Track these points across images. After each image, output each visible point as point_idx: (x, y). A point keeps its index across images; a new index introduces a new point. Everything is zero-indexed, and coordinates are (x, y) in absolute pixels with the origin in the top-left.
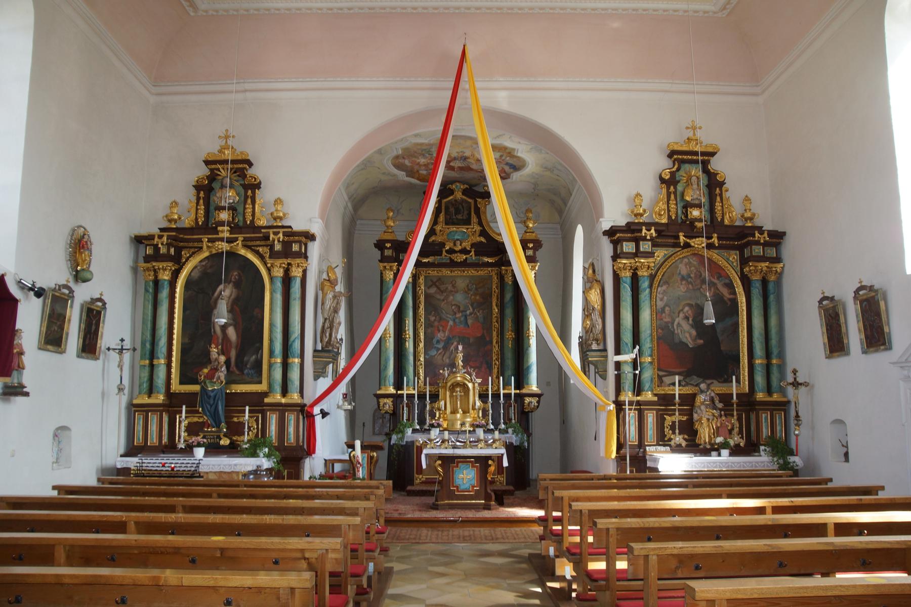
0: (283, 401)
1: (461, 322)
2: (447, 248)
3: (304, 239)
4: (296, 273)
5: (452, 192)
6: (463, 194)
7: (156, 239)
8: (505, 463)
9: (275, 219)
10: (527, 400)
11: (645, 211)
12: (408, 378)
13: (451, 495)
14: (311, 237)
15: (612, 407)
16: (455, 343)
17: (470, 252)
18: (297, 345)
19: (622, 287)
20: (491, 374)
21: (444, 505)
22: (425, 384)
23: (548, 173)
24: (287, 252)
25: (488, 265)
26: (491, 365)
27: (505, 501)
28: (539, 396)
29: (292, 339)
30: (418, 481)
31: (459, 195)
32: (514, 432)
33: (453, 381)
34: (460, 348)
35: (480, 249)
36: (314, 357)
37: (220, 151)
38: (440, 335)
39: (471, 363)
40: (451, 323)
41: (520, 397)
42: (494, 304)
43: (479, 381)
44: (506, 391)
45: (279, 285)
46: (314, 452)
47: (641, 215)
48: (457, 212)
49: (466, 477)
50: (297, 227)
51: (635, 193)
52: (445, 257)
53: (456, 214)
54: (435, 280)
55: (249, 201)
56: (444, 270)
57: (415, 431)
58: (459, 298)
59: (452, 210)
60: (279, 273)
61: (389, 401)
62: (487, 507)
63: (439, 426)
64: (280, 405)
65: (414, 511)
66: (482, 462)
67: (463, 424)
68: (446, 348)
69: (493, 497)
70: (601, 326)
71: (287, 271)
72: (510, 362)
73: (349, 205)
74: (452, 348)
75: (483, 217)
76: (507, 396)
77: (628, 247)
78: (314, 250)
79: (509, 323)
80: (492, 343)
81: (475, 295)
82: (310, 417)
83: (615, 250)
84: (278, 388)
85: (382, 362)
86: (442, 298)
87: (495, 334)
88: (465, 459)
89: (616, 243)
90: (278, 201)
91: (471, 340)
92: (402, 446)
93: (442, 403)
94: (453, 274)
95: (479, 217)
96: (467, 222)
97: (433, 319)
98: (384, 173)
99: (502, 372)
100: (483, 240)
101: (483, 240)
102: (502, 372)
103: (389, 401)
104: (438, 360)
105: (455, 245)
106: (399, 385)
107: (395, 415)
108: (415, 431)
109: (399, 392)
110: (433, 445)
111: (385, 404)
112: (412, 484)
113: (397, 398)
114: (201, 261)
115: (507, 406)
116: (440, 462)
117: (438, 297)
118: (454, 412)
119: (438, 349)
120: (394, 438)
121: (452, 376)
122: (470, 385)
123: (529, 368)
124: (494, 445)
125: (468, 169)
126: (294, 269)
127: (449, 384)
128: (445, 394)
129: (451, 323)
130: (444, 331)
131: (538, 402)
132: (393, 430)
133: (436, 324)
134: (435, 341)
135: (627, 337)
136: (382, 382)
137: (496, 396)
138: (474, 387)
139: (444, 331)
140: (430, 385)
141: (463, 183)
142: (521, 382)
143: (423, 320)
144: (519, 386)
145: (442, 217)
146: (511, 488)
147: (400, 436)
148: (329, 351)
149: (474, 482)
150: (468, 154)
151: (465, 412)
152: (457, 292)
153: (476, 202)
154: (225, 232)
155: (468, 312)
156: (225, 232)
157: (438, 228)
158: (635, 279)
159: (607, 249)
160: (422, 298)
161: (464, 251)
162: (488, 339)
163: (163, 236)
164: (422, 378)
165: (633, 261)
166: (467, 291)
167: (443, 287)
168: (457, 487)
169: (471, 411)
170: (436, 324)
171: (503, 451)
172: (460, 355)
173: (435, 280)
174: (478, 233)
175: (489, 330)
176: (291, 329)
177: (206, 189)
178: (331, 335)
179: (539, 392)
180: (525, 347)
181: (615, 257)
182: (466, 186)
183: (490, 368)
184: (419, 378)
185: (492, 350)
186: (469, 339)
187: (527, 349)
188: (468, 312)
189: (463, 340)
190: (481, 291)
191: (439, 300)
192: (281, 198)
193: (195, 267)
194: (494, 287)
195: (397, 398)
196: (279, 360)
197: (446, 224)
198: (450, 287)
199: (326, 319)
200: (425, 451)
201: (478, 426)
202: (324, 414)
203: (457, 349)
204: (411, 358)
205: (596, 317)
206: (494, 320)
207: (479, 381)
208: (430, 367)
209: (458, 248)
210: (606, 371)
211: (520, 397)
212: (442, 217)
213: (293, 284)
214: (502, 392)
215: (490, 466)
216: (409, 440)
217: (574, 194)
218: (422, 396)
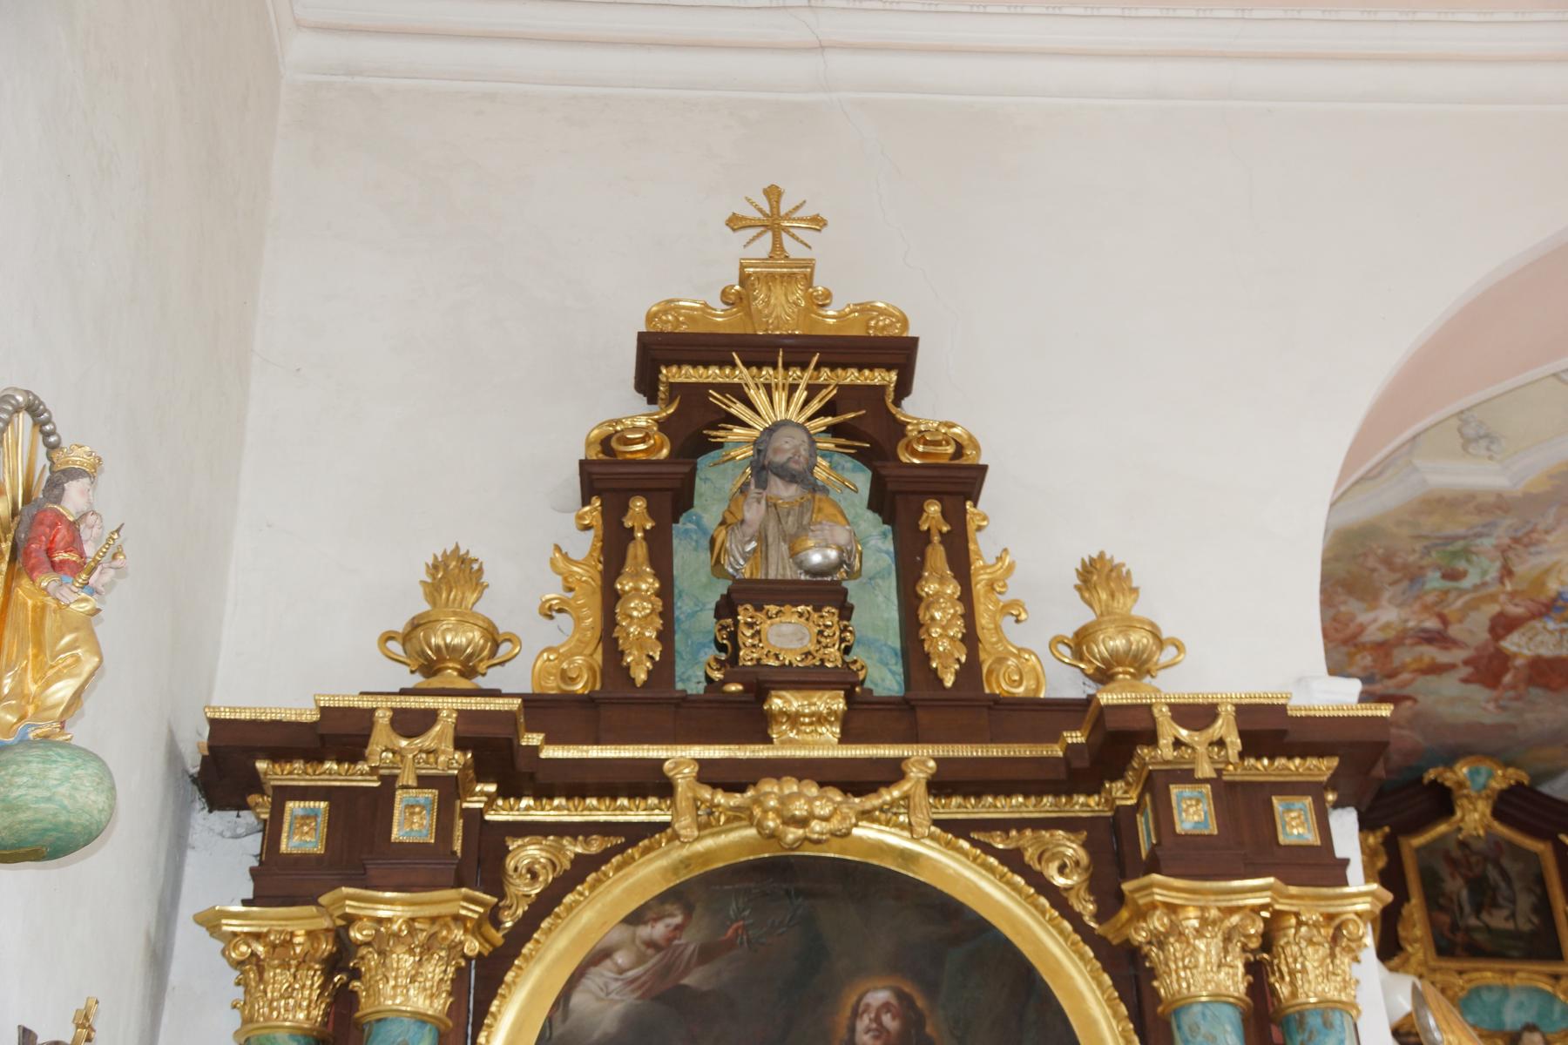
6: (1497, 814)
7: (383, 745)
31: (1474, 817)
37: (738, 299)
48: (1483, 894)
55: (937, 555)
59: (1455, 886)
114: (635, 918)
154: (809, 728)
156: (809, 728)
163: (428, 718)
177: (637, 494)
182: (1515, 775)
192: (1117, 555)
193: (600, 956)
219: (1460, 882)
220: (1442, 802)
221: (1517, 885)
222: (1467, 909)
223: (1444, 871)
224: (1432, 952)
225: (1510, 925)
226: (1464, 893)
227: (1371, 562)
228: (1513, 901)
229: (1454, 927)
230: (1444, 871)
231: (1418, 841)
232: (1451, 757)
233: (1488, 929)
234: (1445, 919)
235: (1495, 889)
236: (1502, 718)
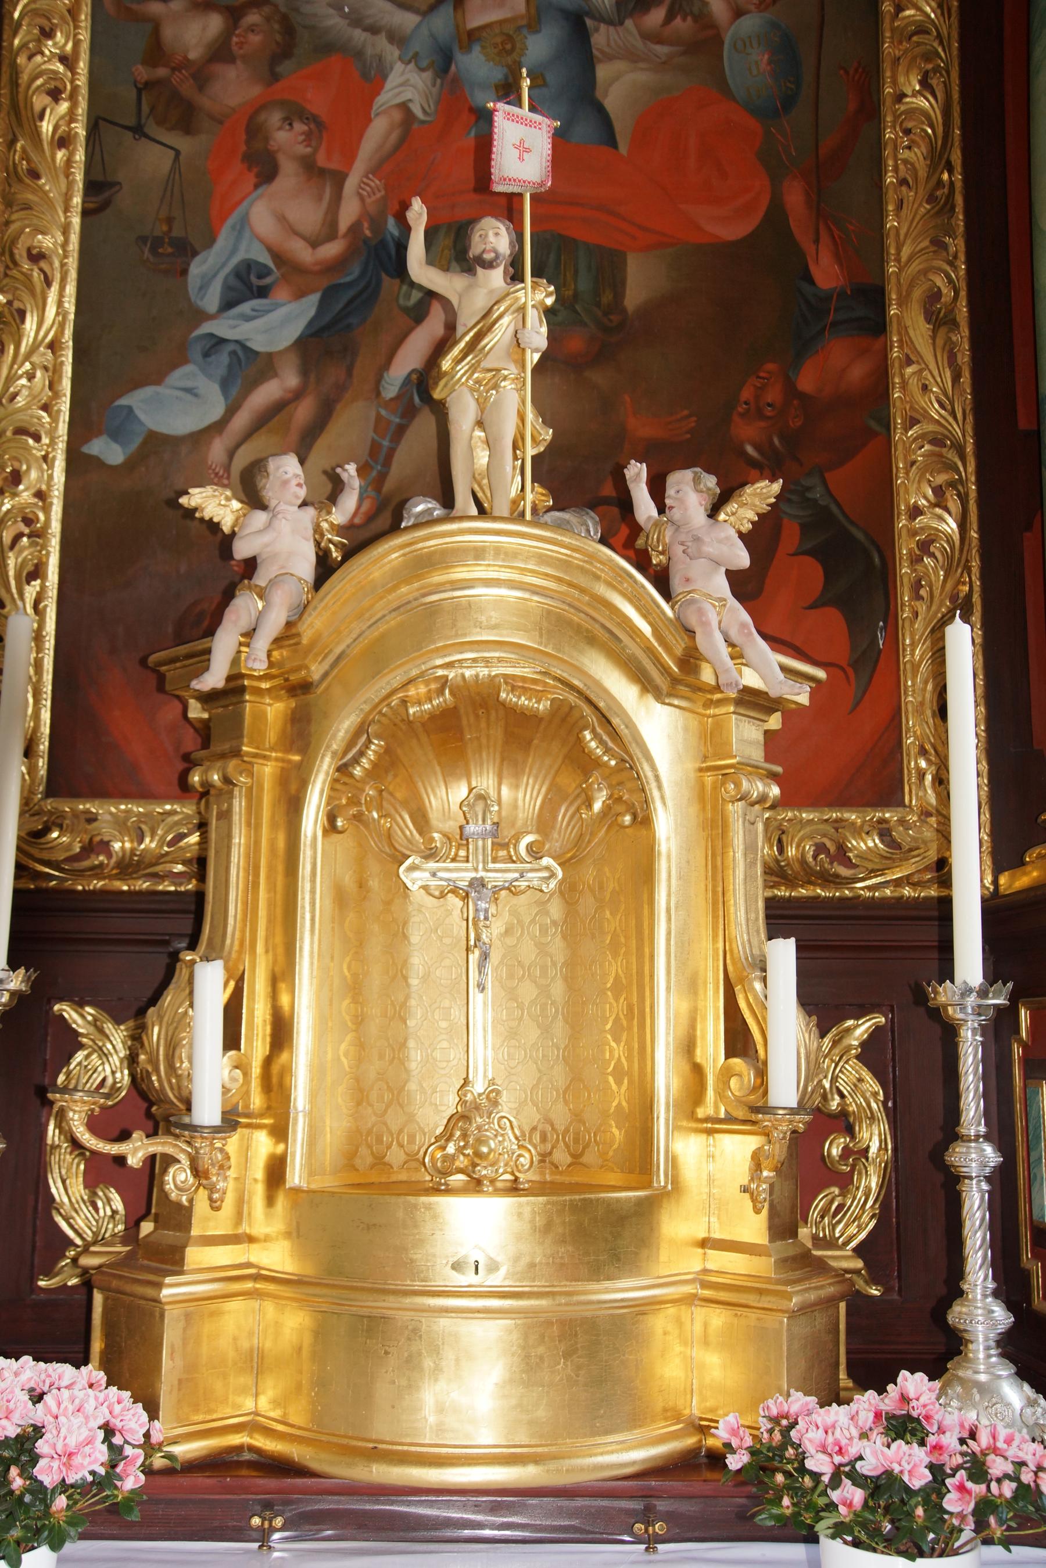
38: (271, 218)
40: (406, 86)
80: (866, 310)
87: (904, 224)
91: (641, 282)
119: (246, 367)
129: (406, 86)
134: (208, 272)
139: (324, 177)
162: (827, 273)
170: (234, 89)
175: (843, 157)
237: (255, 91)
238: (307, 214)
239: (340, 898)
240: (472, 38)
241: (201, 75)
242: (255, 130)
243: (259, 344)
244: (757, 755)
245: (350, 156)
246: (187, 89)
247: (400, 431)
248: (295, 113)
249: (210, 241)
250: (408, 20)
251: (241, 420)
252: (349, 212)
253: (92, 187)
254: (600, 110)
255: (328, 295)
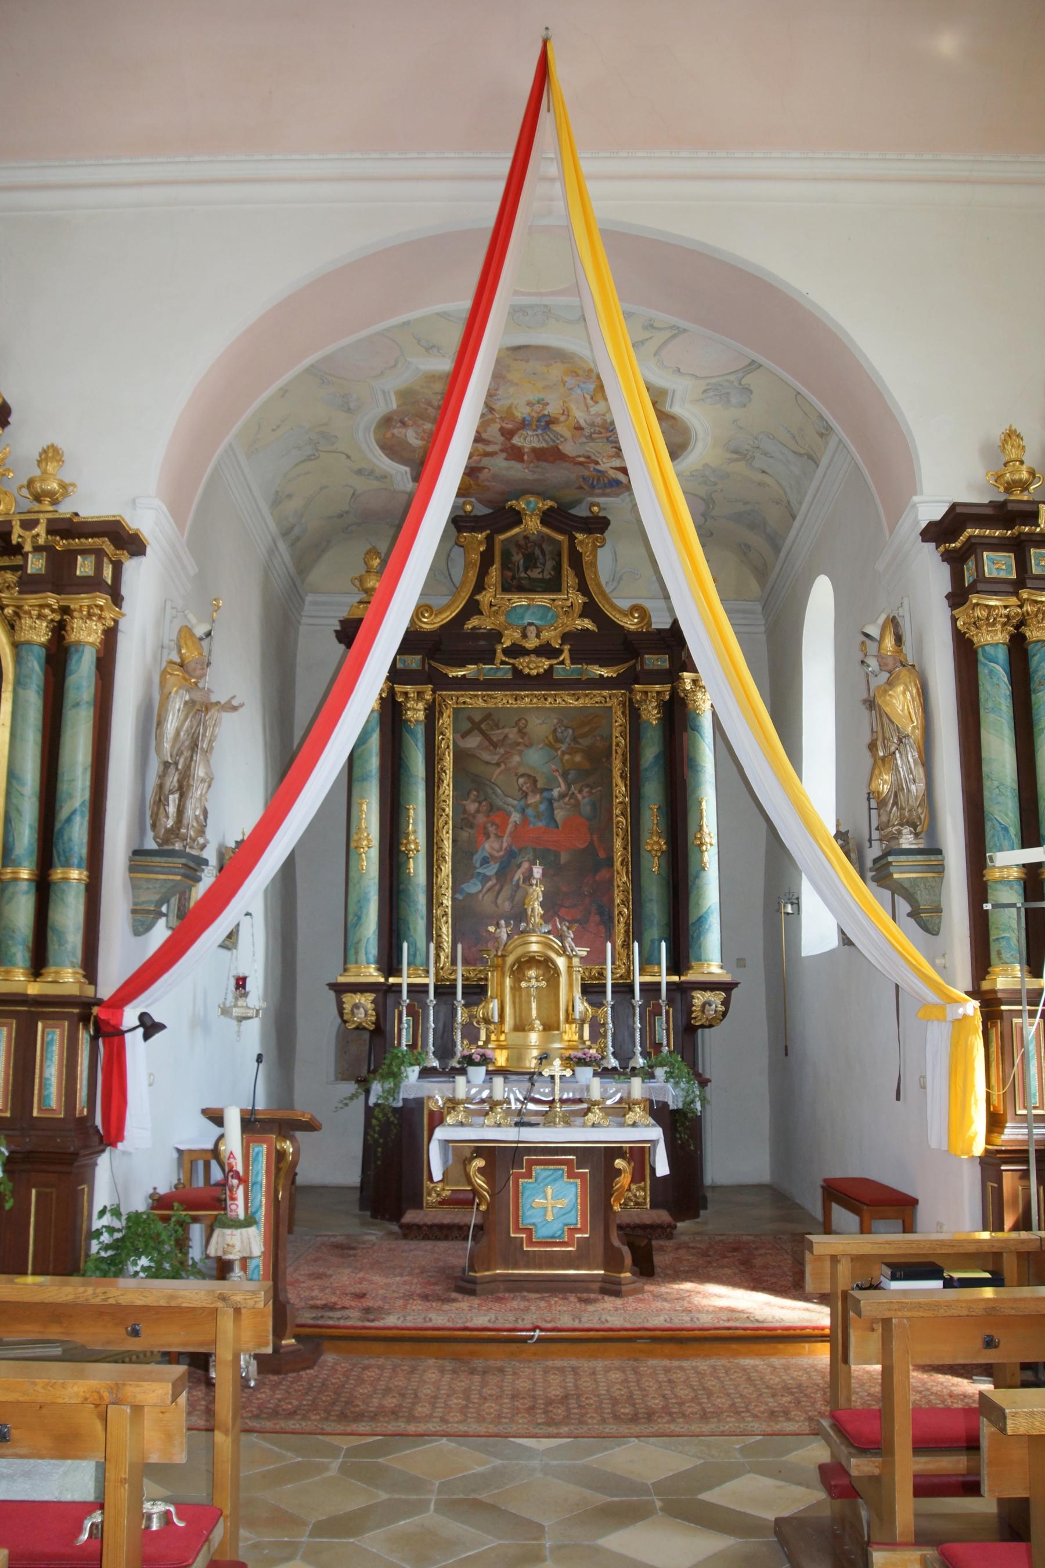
0: (33, 989)
1: (538, 816)
2: (507, 643)
3: (108, 547)
4: (86, 634)
5: (516, 518)
8: (662, 1168)
9: (38, 498)
10: (699, 998)
11: (1032, 473)
12: (413, 946)
13: (514, 1254)
14: (131, 544)
15: (972, 1007)
16: (526, 865)
17: (560, 652)
18: (77, 833)
19: (983, 672)
20: (610, 937)
21: (495, 1279)
22: (454, 962)
23: (740, 467)
24: (60, 577)
25: (602, 683)
26: (611, 918)
27: (658, 1259)
28: (727, 988)
29: (63, 814)
30: (433, 1198)
31: (533, 525)
32: (670, 1075)
33: (519, 951)
34: (537, 871)
35: (583, 647)
36: (133, 869)
38: (490, 846)
39: (563, 912)
40: (515, 817)
41: (681, 992)
42: (616, 773)
43: (583, 952)
44: (648, 979)
45: (35, 667)
46: (119, 1136)
47: (1024, 486)
48: (531, 561)
49: (552, 1205)
50: (90, 505)
51: (1004, 428)
52: (499, 668)
53: (526, 570)
54: (477, 718)
56: (498, 693)
57: (426, 1073)
58: (535, 758)
59: (518, 558)
60: (38, 633)
61: (366, 1000)
62: (611, 1289)
63: (485, 1060)
64: (22, 999)
65: (408, 1297)
66: (599, 1163)
67: (544, 1058)
68: (504, 873)
69: (628, 1259)
70: (922, 785)
71: (59, 630)
72: (655, 909)
73: (282, 546)
74: (519, 875)
75: (589, 575)
76: (651, 990)
77: (998, 565)
78: (141, 579)
79: (652, 818)
80: (610, 862)
81: (572, 751)
82: (109, 1035)
83: (957, 577)
84: (21, 954)
85: (352, 908)
86: (495, 759)
87: (618, 844)
88: (549, 1153)
89: (955, 560)
90: (51, 454)
91: (564, 858)
92: (395, 1110)
93: (494, 1005)
94: (521, 704)
95: (580, 574)
96: (554, 585)
97: (472, 807)
98: (360, 472)
99: (636, 931)
100: (588, 624)
101: (588, 624)
102: (636, 931)
103: (366, 1000)
104: (486, 902)
105: (524, 636)
106: (390, 964)
107: (380, 1033)
108: (426, 1073)
109: (392, 980)
110: (466, 1117)
111: (356, 1006)
112: (417, 1203)
113: (385, 993)
115: (651, 1012)
116: (480, 1163)
117: (486, 756)
118: (522, 1026)
119: (485, 879)
120: (377, 1088)
121: (517, 939)
122: (561, 962)
123: (701, 920)
124: (631, 1117)
125: (552, 455)
126: (77, 623)
127: (510, 960)
128: (502, 984)
129: (515, 817)
130: (499, 837)
131: (726, 1003)
132: (374, 1072)
133: (481, 819)
134: (477, 858)
135: (1003, 808)
136: (351, 952)
137: (623, 989)
138: (570, 967)
139: (499, 837)
140: (466, 962)
141: (543, 495)
142: (682, 952)
143: (449, 810)
144: (678, 963)
145: (494, 573)
146: (663, 1216)
147: (389, 1084)
148: (172, 853)
149: (575, 1218)
150: (553, 409)
151: (550, 1027)
152: (529, 746)
153: (572, 539)
155: (555, 793)
157: (485, 598)
158: (1018, 648)
159: (931, 574)
160: (448, 761)
161: (546, 651)
162: (602, 855)
164: (447, 946)
165: (1013, 600)
166: (553, 743)
167: (496, 735)
168: (529, 1231)
169: (564, 1026)
170: (481, 819)
171: (656, 1133)
172: (537, 892)
173: (477, 718)
174: (577, 610)
175: (604, 829)
176: (63, 787)
178: (180, 811)
179: (727, 978)
180: (692, 869)
181: (958, 597)
182: (550, 503)
183: (607, 921)
184: (439, 947)
185: (611, 881)
186: (557, 856)
187: (697, 877)
188: (555, 793)
189: (546, 856)
190: (585, 742)
191: (487, 763)
192: (59, 444)
194: (616, 733)
195: (385, 993)
196: (25, 874)
197: (506, 589)
198: (513, 734)
199: (166, 765)
200: (440, 1133)
201: (582, 1062)
202: (150, 1027)
203: (529, 875)
204: (421, 899)
205: (908, 760)
206: (617, 811)
207: (583, 952)
208: (468, 923)
209: (532, 643)
210: (938, 910)
211: (681, 992)
212: (494, 573)
213: (72, 664)
214: (638, 979)
215: (619, 1172)
216: (412, 1096)
217: (799, 519)
218: (445, 991)
219: (521, 555)
220: (516, 518)
221: (547, 557)
222: (521, 569)
223: (514, 551)
224: (499, 589)
225: (540, 576)
226: (522, 562)
227: (423, 406)
228: (544, 565)
229: (513, 578)
230: (514, 551)
231: (502, 537)
232: (518, 495)
233: (529, 578)
234: (510, 574)
235: (536, 559)
236: (536, 476)
237: (485, 819)
238: (496, 846)
239: (511, 988)
240: (528, 806)
241: (474, 817)
242: (485, 828)
243: (488, 874)
244: (578, 964)
245: (504, 832)
246: (471, 819)
247: (516, 891)
248: (493, 824)
249: (477, 852)
250: (515, 802)
251: (485, 889)
252: (505, 845)
253: (453, 841)
254: (555, 821)
255: (501, 863)
